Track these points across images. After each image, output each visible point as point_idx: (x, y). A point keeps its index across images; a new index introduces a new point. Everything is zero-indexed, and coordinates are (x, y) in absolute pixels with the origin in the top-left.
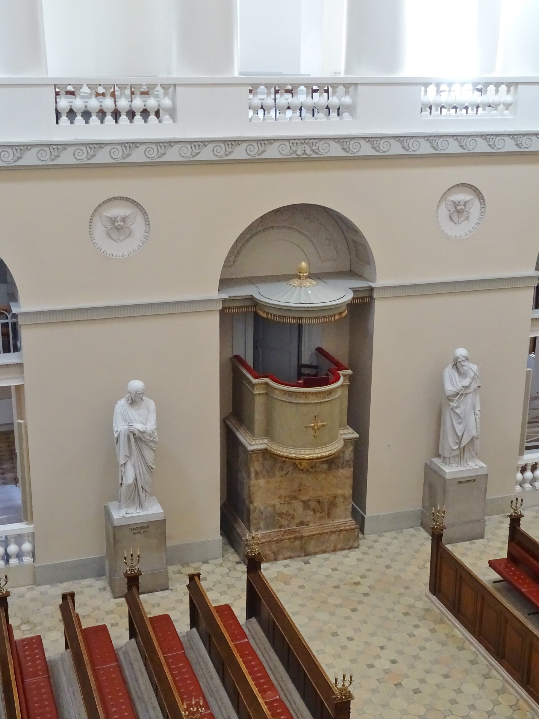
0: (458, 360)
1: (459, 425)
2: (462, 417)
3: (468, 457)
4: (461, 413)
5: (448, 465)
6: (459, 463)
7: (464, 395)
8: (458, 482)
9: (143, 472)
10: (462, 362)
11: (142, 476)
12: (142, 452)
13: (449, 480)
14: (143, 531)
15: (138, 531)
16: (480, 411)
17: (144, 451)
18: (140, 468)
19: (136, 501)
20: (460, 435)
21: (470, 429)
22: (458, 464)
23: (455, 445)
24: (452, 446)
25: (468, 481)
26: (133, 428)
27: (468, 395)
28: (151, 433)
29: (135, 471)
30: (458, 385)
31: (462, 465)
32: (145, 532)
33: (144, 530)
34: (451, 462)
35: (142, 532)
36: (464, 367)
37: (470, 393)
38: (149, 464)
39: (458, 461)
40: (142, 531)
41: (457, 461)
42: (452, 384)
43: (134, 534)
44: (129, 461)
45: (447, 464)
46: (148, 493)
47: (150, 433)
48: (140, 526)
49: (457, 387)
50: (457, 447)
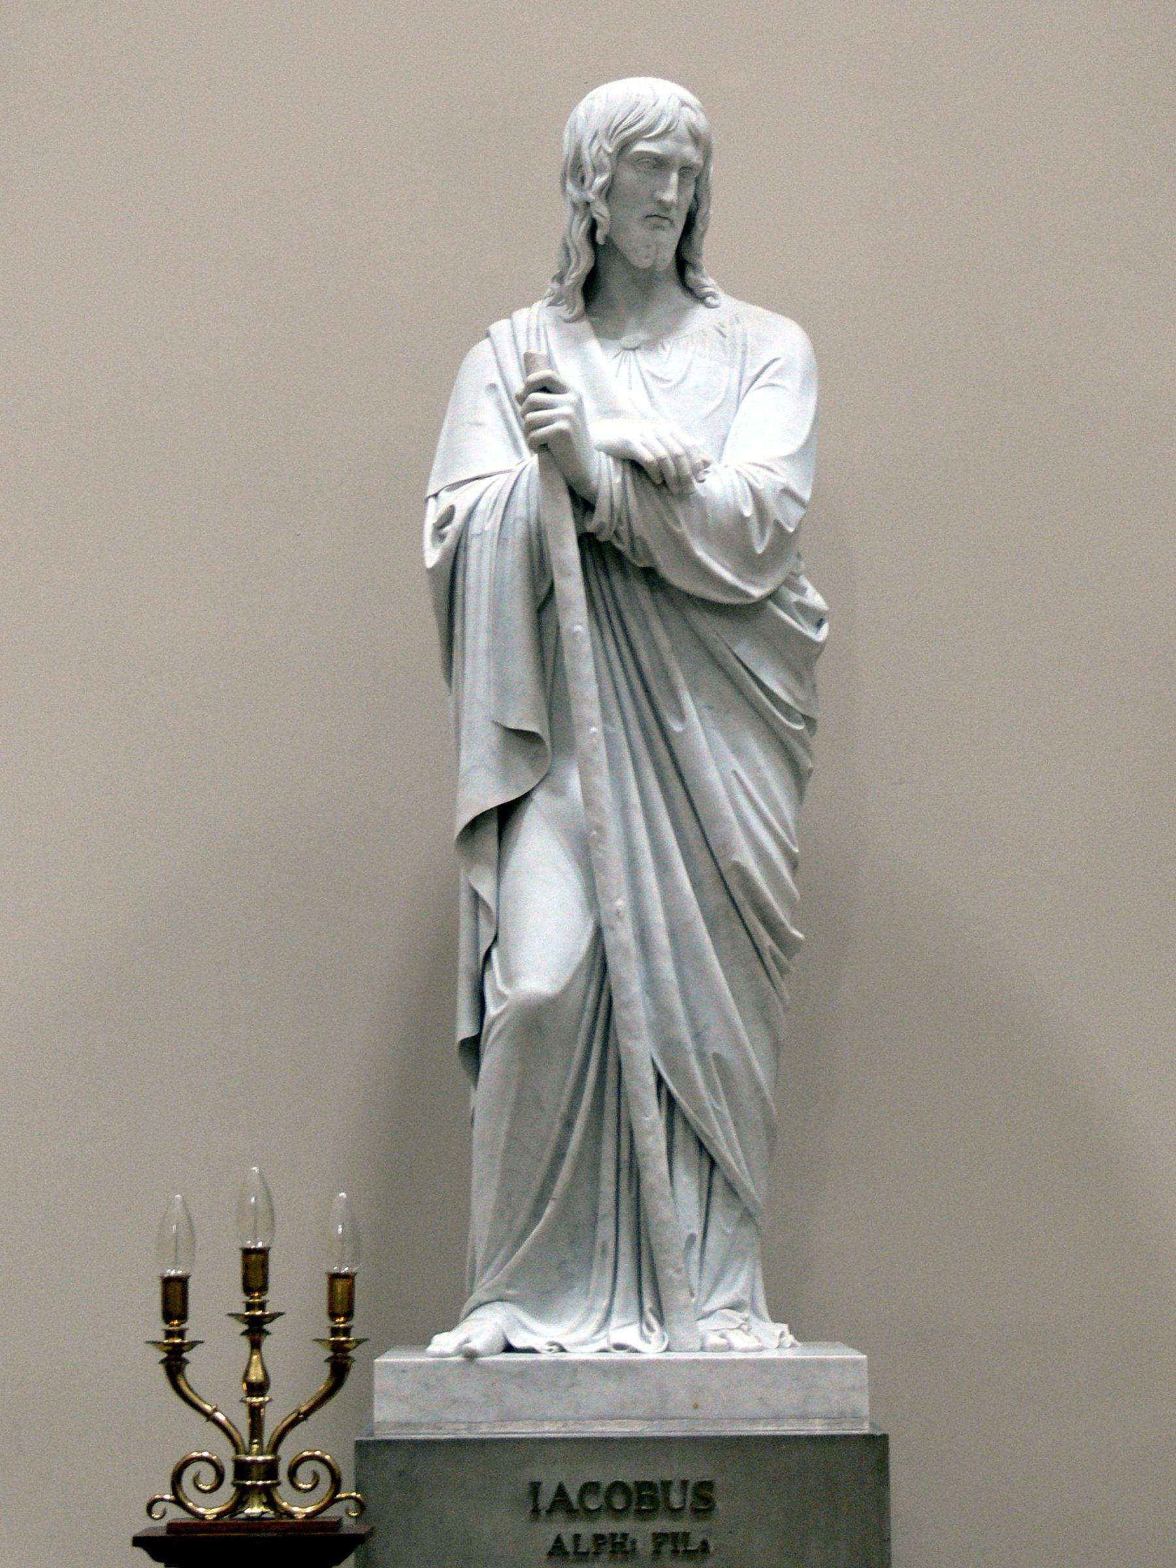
9: (672, 934)
11: (667, 967)
12: (676, 727)
14: (659, 1539)
15: (605, 1526)
17: (682, 716)
18: (650, 878)
19: (605, 1230)
26: (567, 410)
28: (748, 512)
29: (593, 896)
32: (678, 1539)
33: (663, 1524)
35: (645, 1546)
38: (736, 858)
40: (641, 1531)
43: (557, 1549)
44: (539, 797)
46: (732, 1190)
47: (743, 520)
48: (629, 1474)
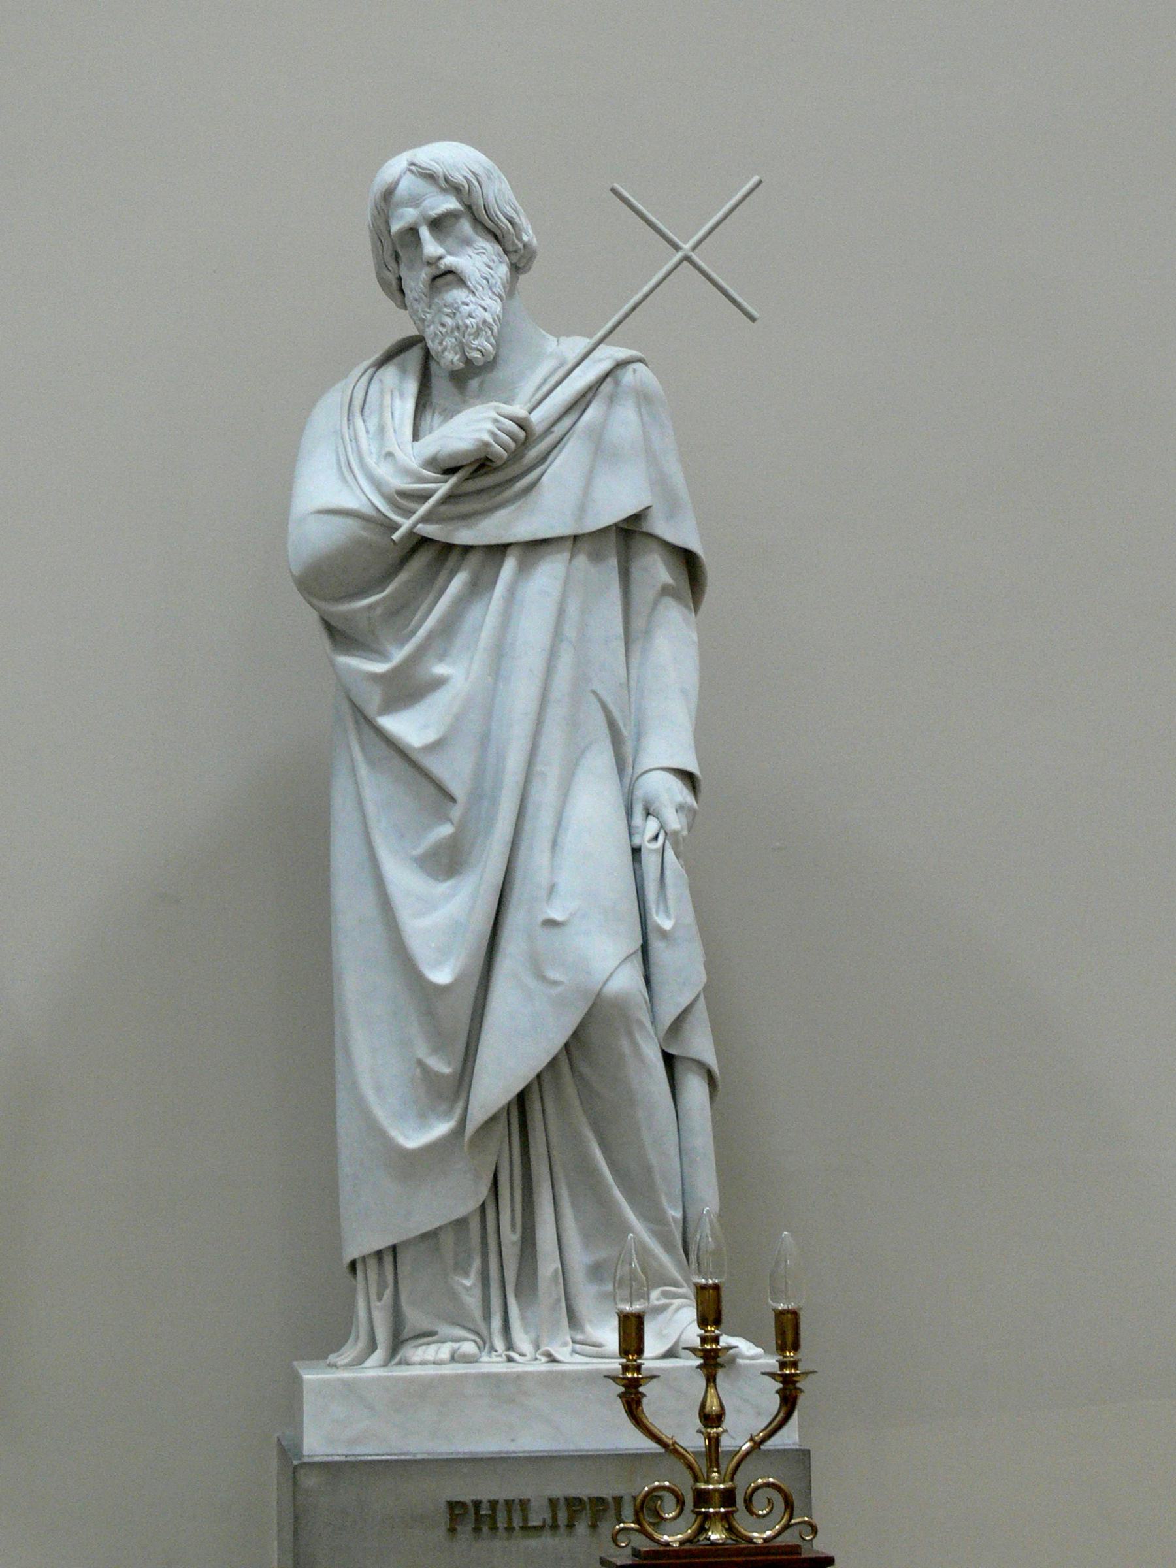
0: (396, 227)
1: (444, 887)
2: (458, 789)
3: (579, 1258)
4: (435, 747)
5: (379, 1355)
6: (496, 1323)
7: (474, 559)
8: (456, 1509)
10: (425, 233)
13: (327, 1467)
16: (688, 777)
20: (441, 976)
21: (551, 923)
22: (485, 1343)
23: (423, 1117)
24: (382, 1115)
25: (575, 1505)
27: (510, 565)
30: (390, 455)
31: (522, 1340)
34: (415, 1318)
36: (458, 295)
37: (537, 547)
39: (487, 1317)
41: (472, 1302)
42: (345, 470)
45: (372, 1346)
49: (384, 471)
50: (441, 1129)
